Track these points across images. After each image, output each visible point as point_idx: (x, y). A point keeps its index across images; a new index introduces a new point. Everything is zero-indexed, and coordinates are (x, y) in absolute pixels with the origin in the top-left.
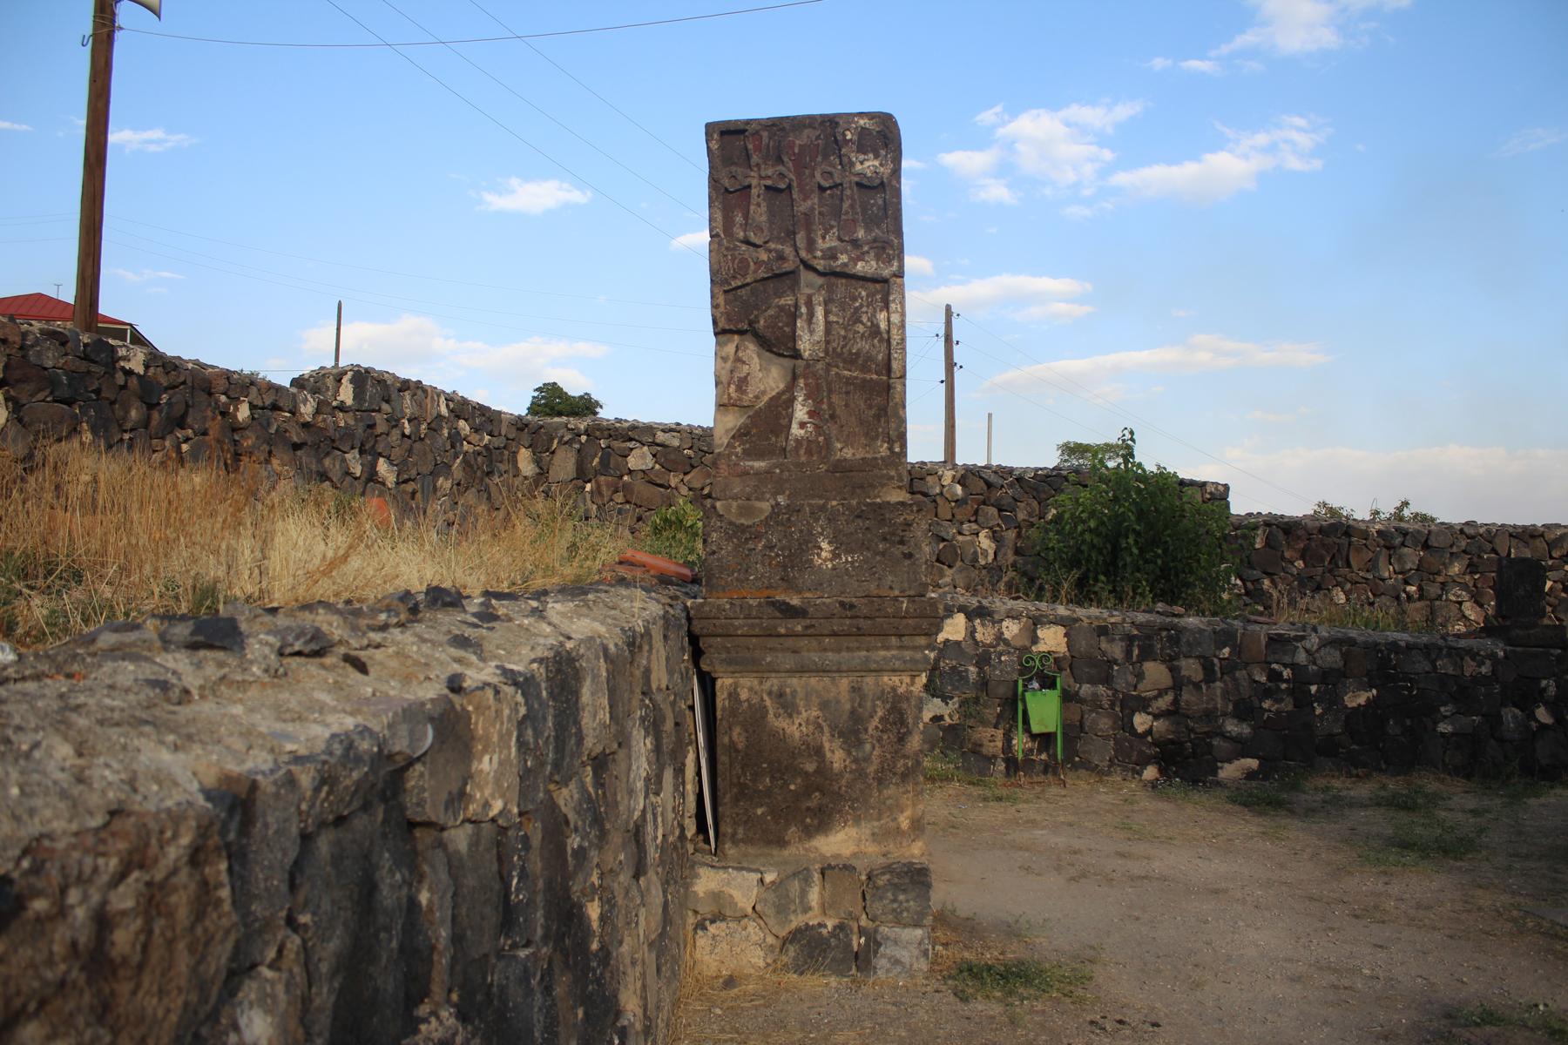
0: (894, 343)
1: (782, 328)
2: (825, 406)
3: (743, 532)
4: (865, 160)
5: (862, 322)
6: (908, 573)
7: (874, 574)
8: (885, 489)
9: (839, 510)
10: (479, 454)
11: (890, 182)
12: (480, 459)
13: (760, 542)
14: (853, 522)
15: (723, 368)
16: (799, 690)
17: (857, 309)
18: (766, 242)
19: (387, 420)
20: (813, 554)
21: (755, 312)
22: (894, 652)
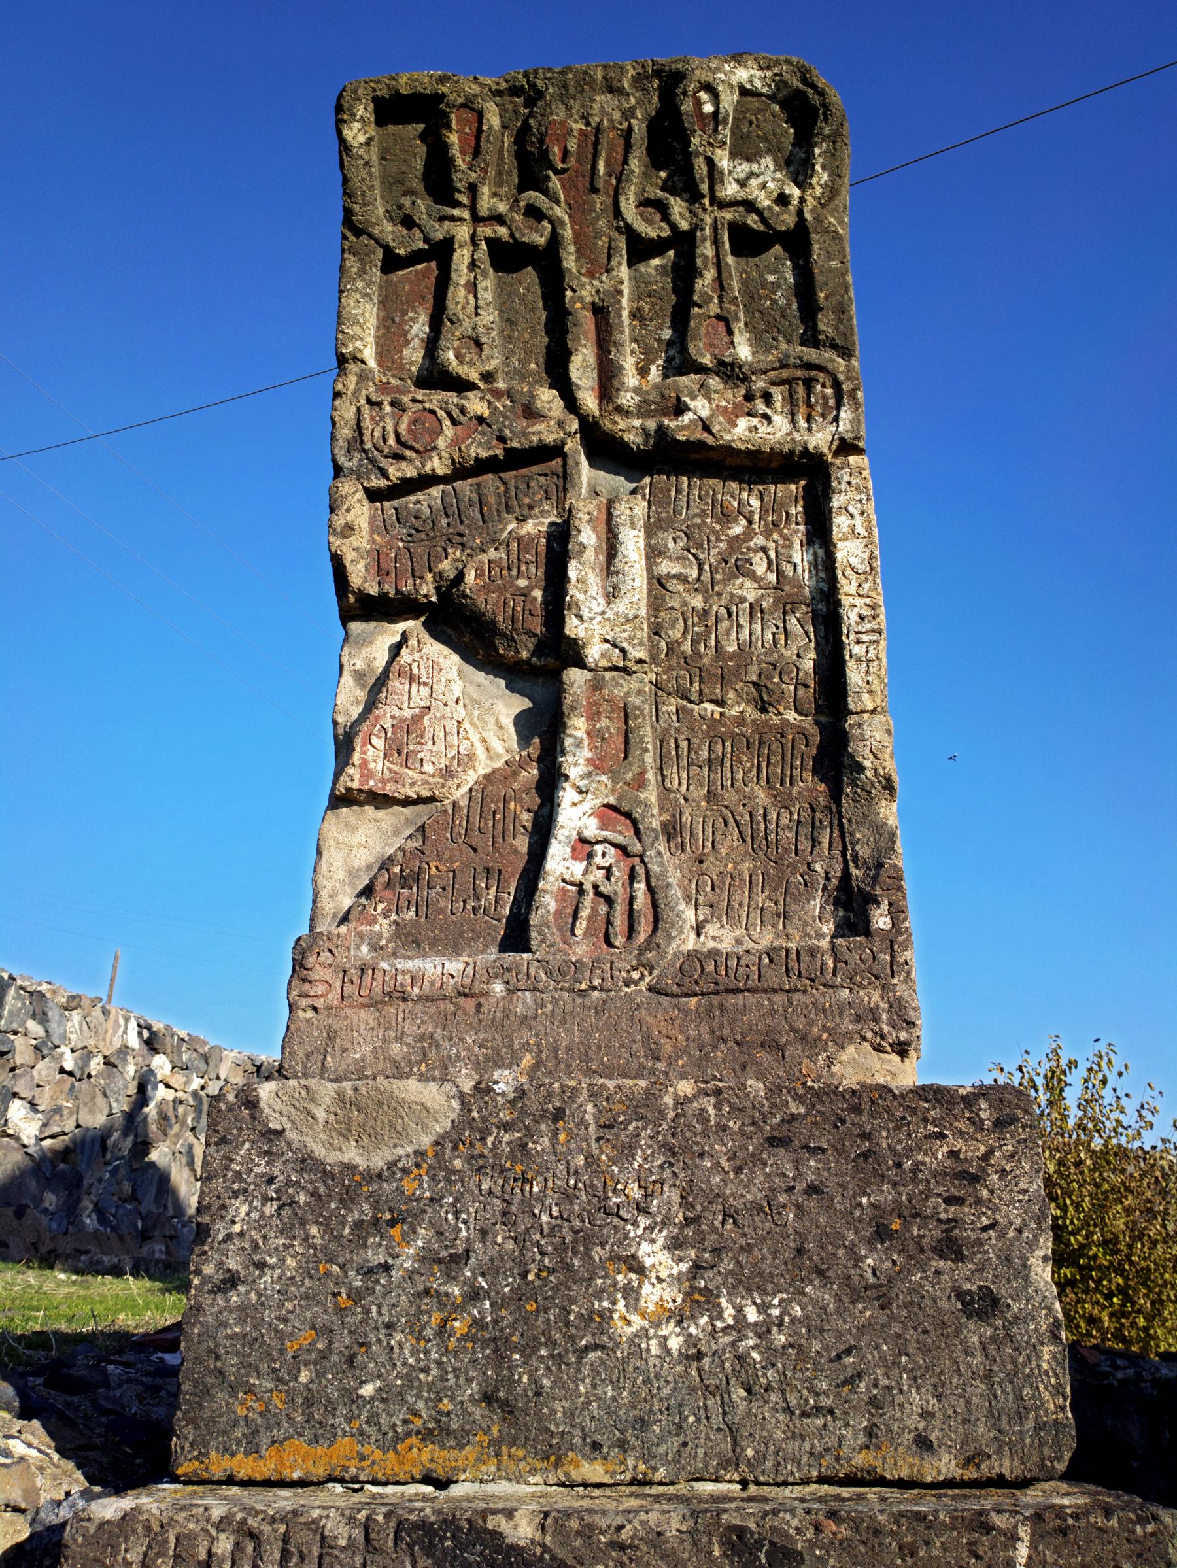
0: (850, 617)
3: (348, 1199)
4: (751, 175)
5: (753, 576)
6: (988, 1376)
8: (851, 1049)
9: (702, 1115)
10: (181, 1103)
11: (819, 219)
12: (181, 1109)
13: (408, 1238)
14: (756, 1159)
19: (36, 1048)
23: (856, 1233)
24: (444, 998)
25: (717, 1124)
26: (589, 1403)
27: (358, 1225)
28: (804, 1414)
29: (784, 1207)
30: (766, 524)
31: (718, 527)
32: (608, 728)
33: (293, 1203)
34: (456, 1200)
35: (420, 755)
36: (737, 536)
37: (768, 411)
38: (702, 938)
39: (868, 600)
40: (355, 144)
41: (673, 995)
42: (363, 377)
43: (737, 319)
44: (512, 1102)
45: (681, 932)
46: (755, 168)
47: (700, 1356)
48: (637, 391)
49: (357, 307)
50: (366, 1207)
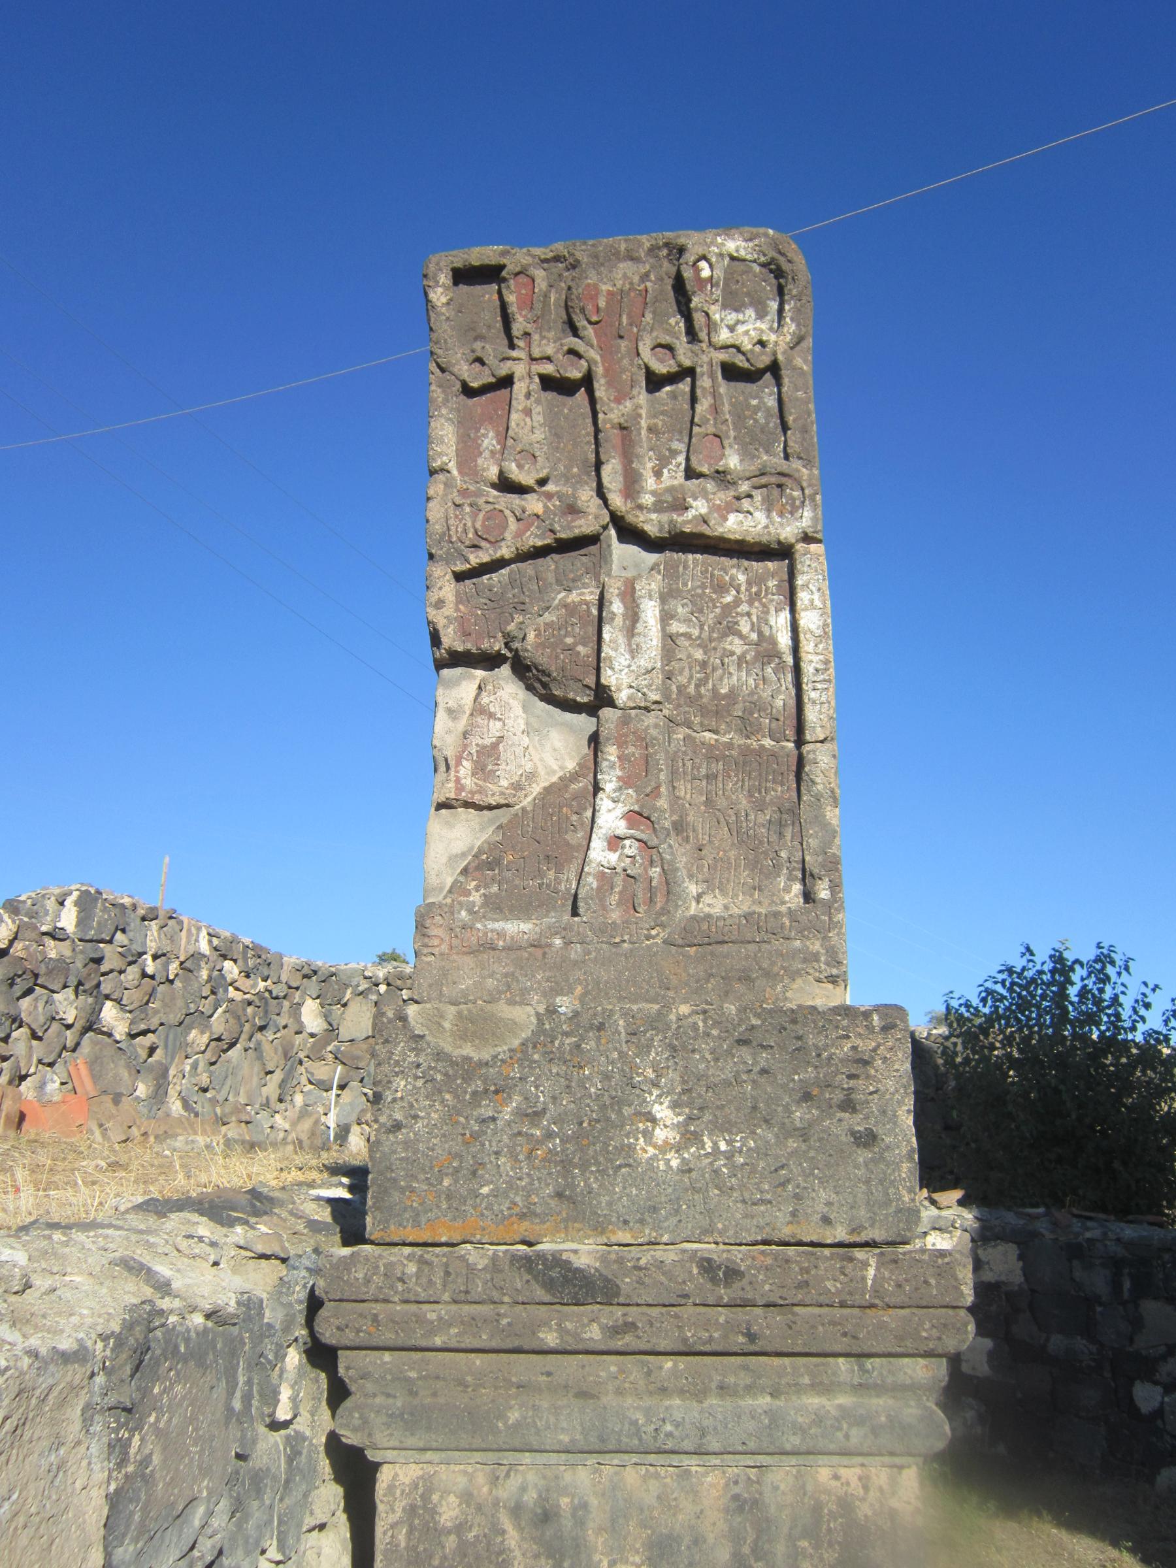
0: (808, 669)
1: (570, 649)
2: (663, 803)
3: (468, 1078)
4: (738, 322)
7: (782, 1185)
8: (799, 981)
9: (695, 1026)
10: (250, 1004)
11: (789, 360)
12: (250, 1010)
14: (729, 1053)
15: (449, 732)
16: (594, 1502)
17: (727, 609)
18: (542, 482)
20: (634, 1133)
21: (518, 618)
22: (844, 1400)
23: (790, 1096)
24: (520, 948)
25: (704, 1032)
26: (621, 1197)
27: (474, 1093)
28: (754, 1204)
29: (745, 1082)
30: (750, 595)
31: (714, 596)
32: (633, 755)
33: (433, 1080)
34: (536, 1079)
35: (498, 773)
36: (728, 604)
37: (751, 510)
38: (701, 905)
39: (821, 657)
40: (439, 304)
41: (679, 946)
42: (448, 485)
43: (728, 438)
44: (570, 1019)
45: (685, 902)
46: (741, 317)
47: (690, 1171)
48: (653, 493)
49: (442, 429)
50: (479, 1082)
